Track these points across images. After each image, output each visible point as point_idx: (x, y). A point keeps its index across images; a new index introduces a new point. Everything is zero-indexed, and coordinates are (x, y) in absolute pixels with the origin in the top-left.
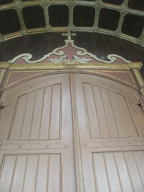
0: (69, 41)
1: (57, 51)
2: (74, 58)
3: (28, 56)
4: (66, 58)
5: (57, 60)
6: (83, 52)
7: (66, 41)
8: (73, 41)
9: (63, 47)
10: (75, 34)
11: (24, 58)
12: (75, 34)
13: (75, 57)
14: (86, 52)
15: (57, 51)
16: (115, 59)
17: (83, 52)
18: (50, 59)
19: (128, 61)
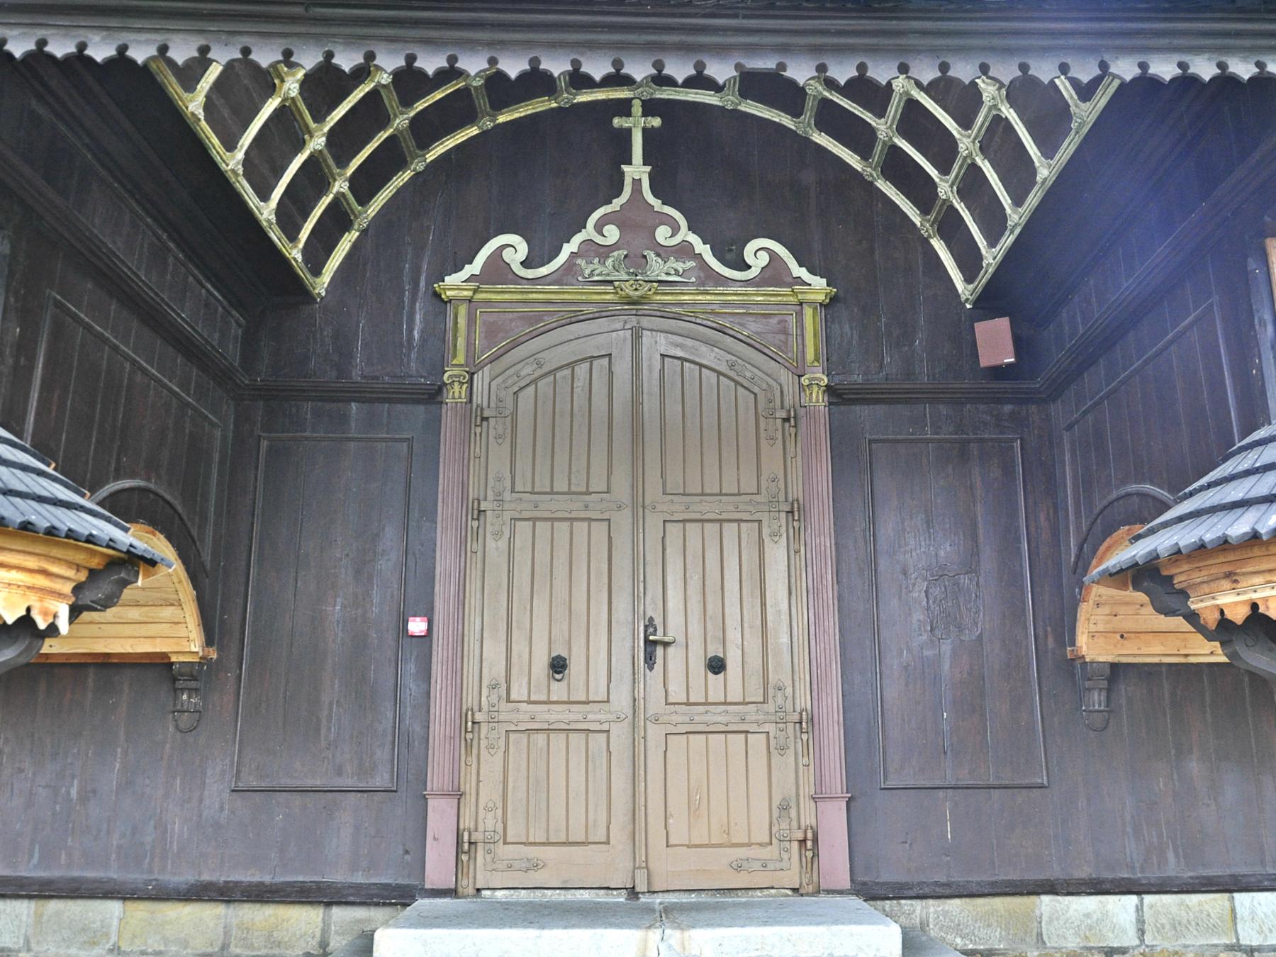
0: (637, 170)
1: (599, 228)
2: (645, 257)
3: (515, 247)
4: (626, 256)
5: (600, 269)
6: (676, 230)
7: (625, 168)
8: (648, 168)
9: (617, 203)
10: (656, 122)
11: (507, 255)
12: (656, 122)
13: (651, 255)
14: (686, 235)
15: (599, 228)
16: (764, 259)
17: (676, 230)
18: (579, 261)
19: (802, 273)
